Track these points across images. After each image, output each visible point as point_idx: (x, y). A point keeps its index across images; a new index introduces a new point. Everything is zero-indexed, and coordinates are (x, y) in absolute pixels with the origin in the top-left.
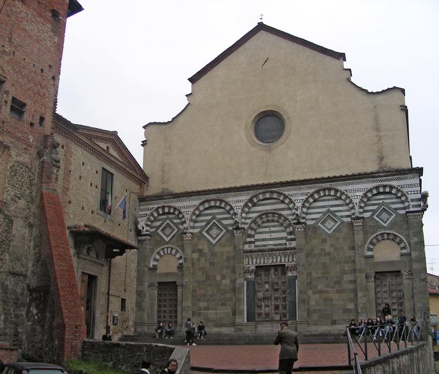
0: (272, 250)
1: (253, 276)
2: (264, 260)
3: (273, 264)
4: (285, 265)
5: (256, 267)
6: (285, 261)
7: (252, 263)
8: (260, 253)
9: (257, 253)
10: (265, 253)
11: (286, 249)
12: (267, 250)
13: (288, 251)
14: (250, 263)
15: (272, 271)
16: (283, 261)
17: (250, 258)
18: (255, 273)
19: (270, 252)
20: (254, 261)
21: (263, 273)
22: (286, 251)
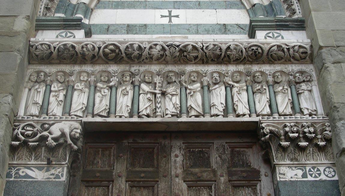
0: (183, 55)
1: (61, 173)
2: (135, 101)
3: (184, 119)
4: (256, 124)
5: (86, 126)
6: (252, 110)
7: (67, 111)
8: (113, 68)
9: (98, 68)
10: (143, 68)
11: (256, 56)
12: (155, 52)
13: (267, 68)
14: (56, 109)
15: (177, 158)
16: (242, 108)
17: (55, 87)
18: (75, 155)
19: (176, 68)
20: (79, 100)
21: (120, 168)
22: (255, 68)
